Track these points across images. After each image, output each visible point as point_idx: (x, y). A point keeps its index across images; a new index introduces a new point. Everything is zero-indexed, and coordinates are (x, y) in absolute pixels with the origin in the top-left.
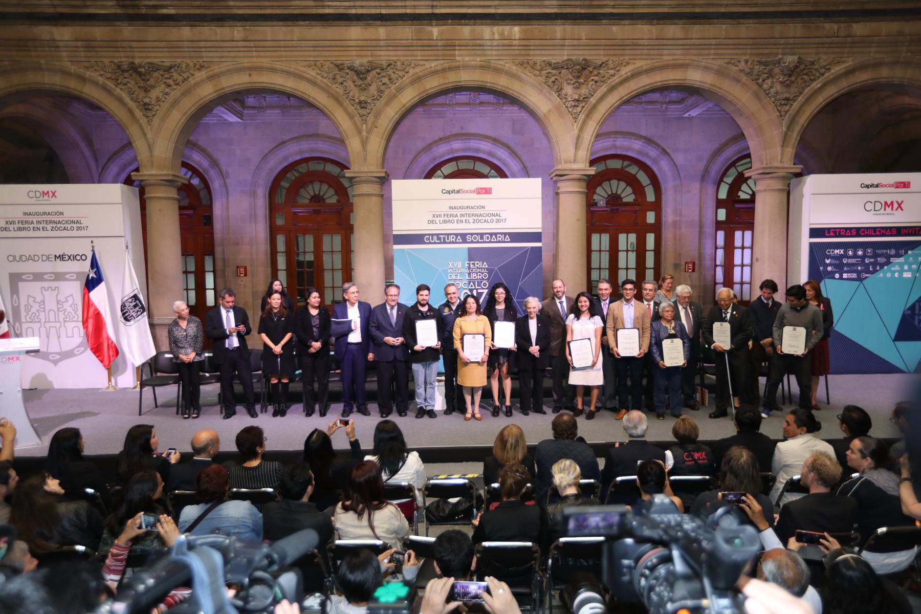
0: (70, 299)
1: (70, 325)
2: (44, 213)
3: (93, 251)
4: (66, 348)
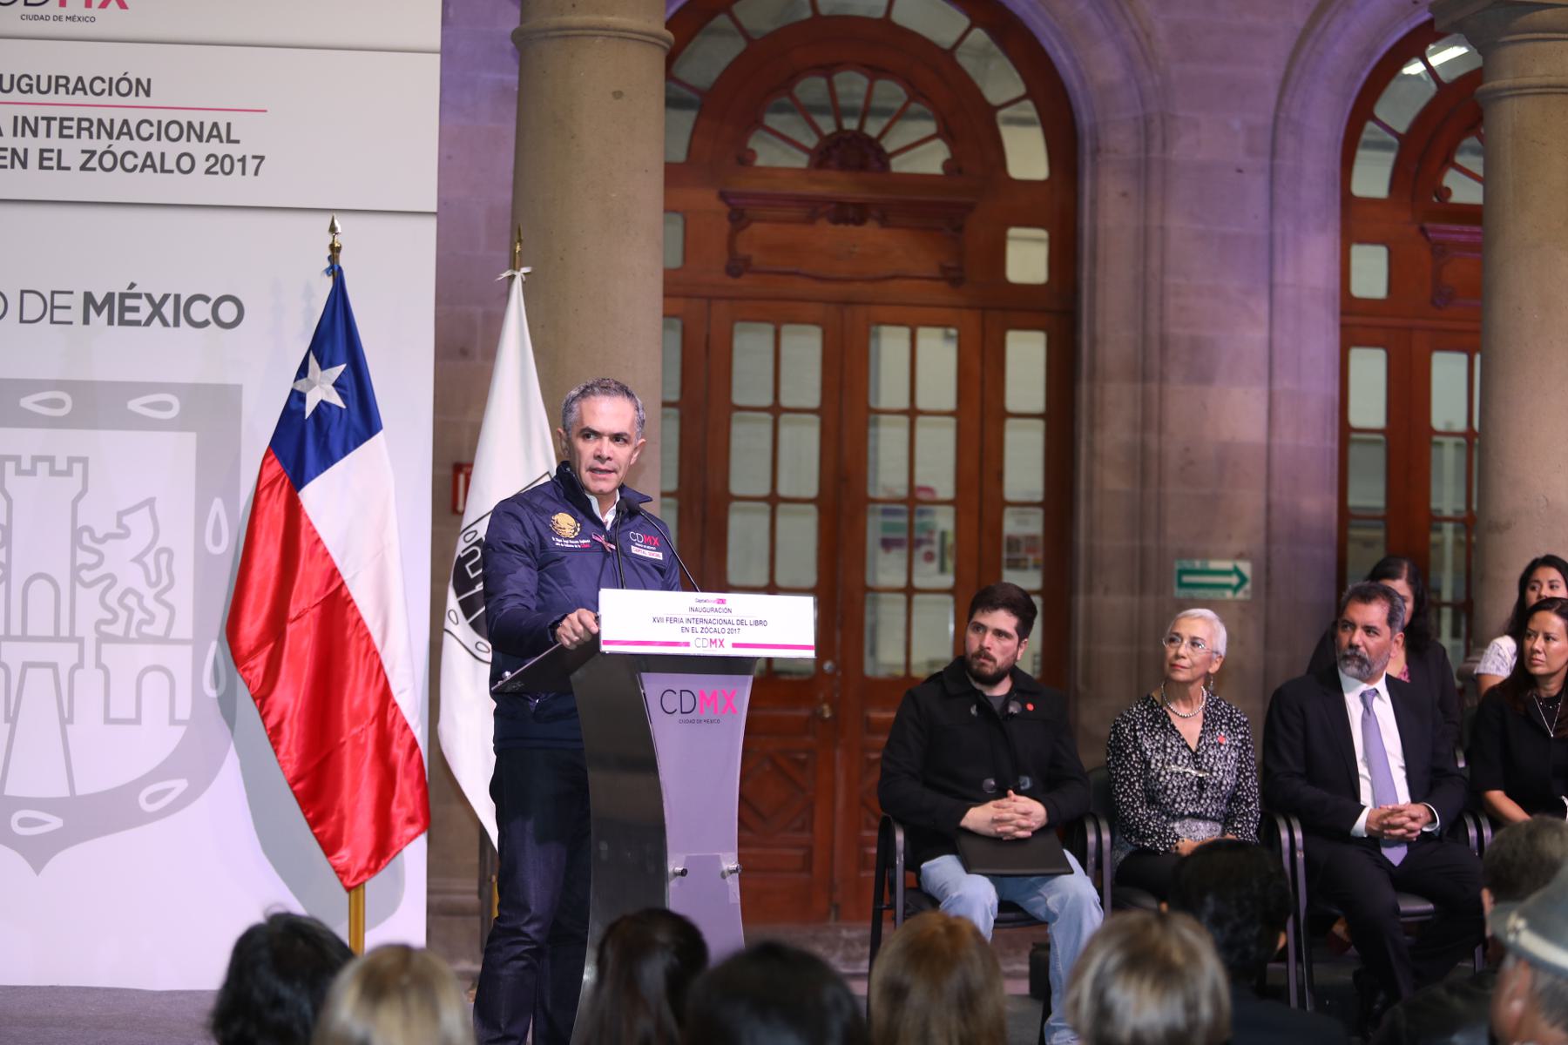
0: (139, 523)
1: (127, 660)
2: (58, 83)
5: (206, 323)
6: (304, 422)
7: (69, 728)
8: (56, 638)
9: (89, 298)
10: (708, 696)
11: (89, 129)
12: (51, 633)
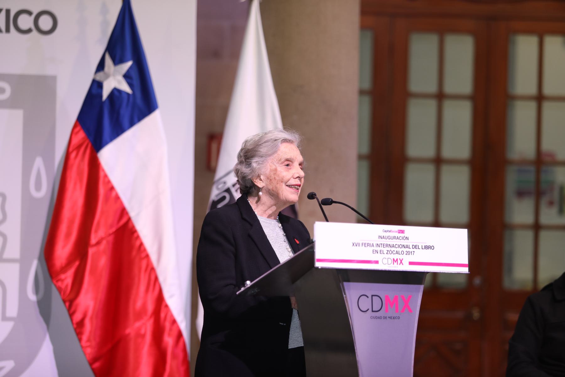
5: (29, 31)
6: (102, 103)
10: (392, 299)
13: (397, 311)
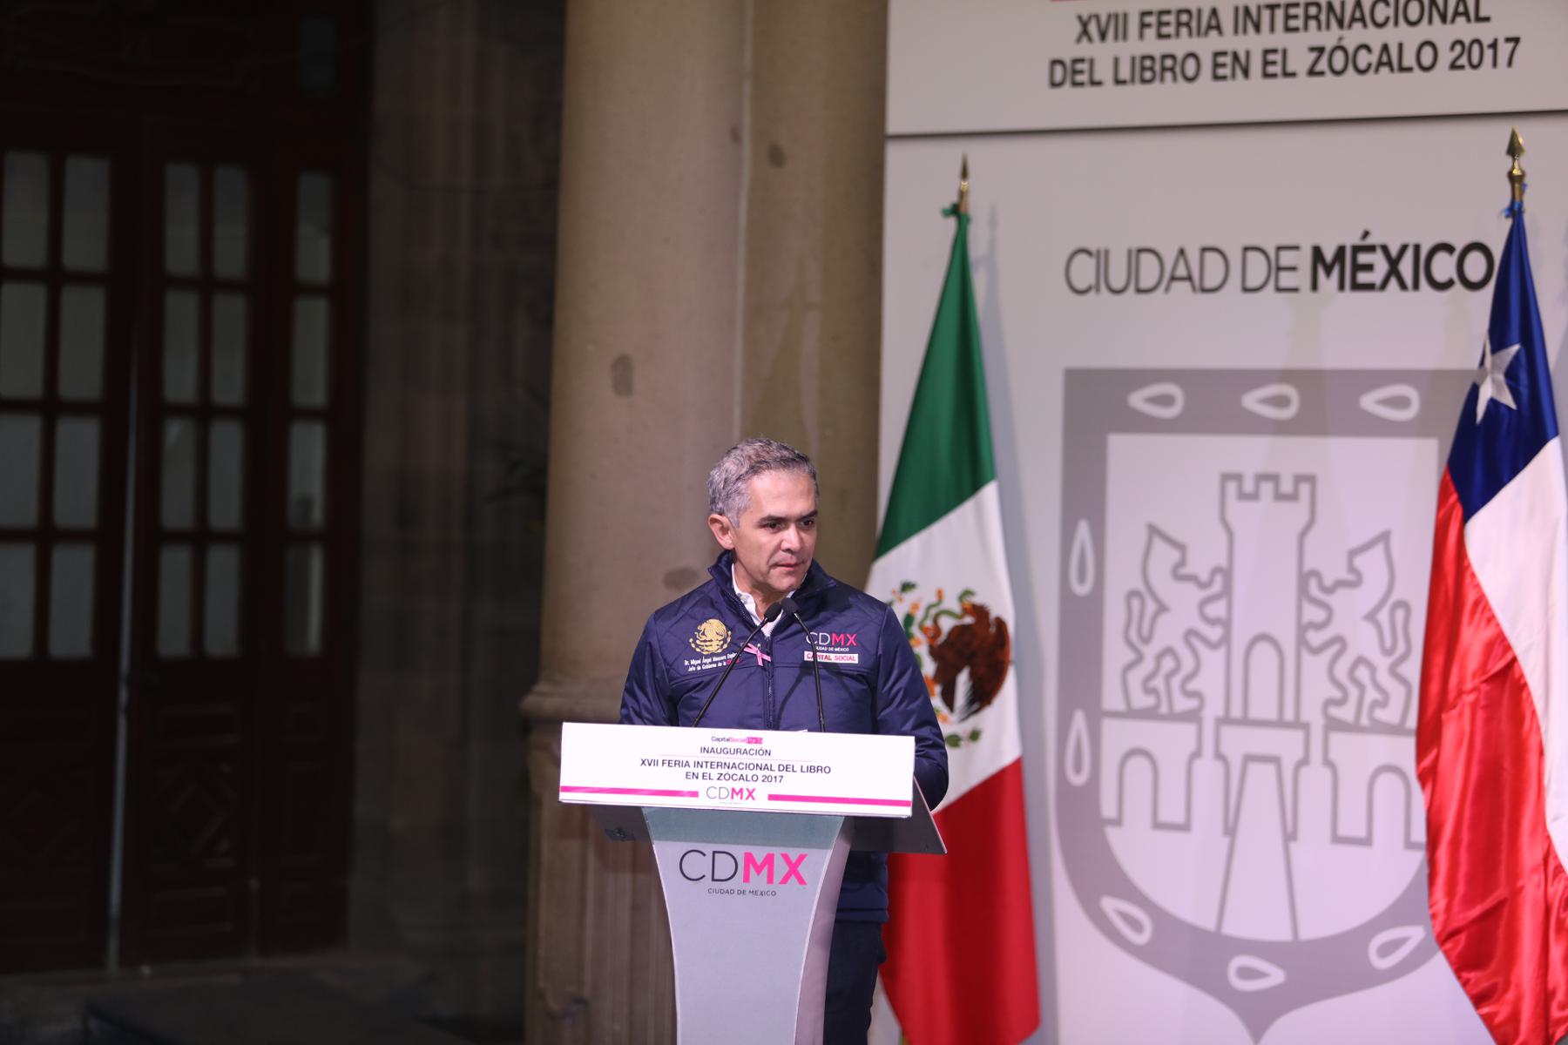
0: (1372, 565)
3: (1515, 212)
4: (1325, 919)
5: (1448, 285)
7: (1293, 846)
8: (1280, 723)
9: (1317, 253)
11: (1317, 18)
12: (1272, 714)
13: (770, 880)
